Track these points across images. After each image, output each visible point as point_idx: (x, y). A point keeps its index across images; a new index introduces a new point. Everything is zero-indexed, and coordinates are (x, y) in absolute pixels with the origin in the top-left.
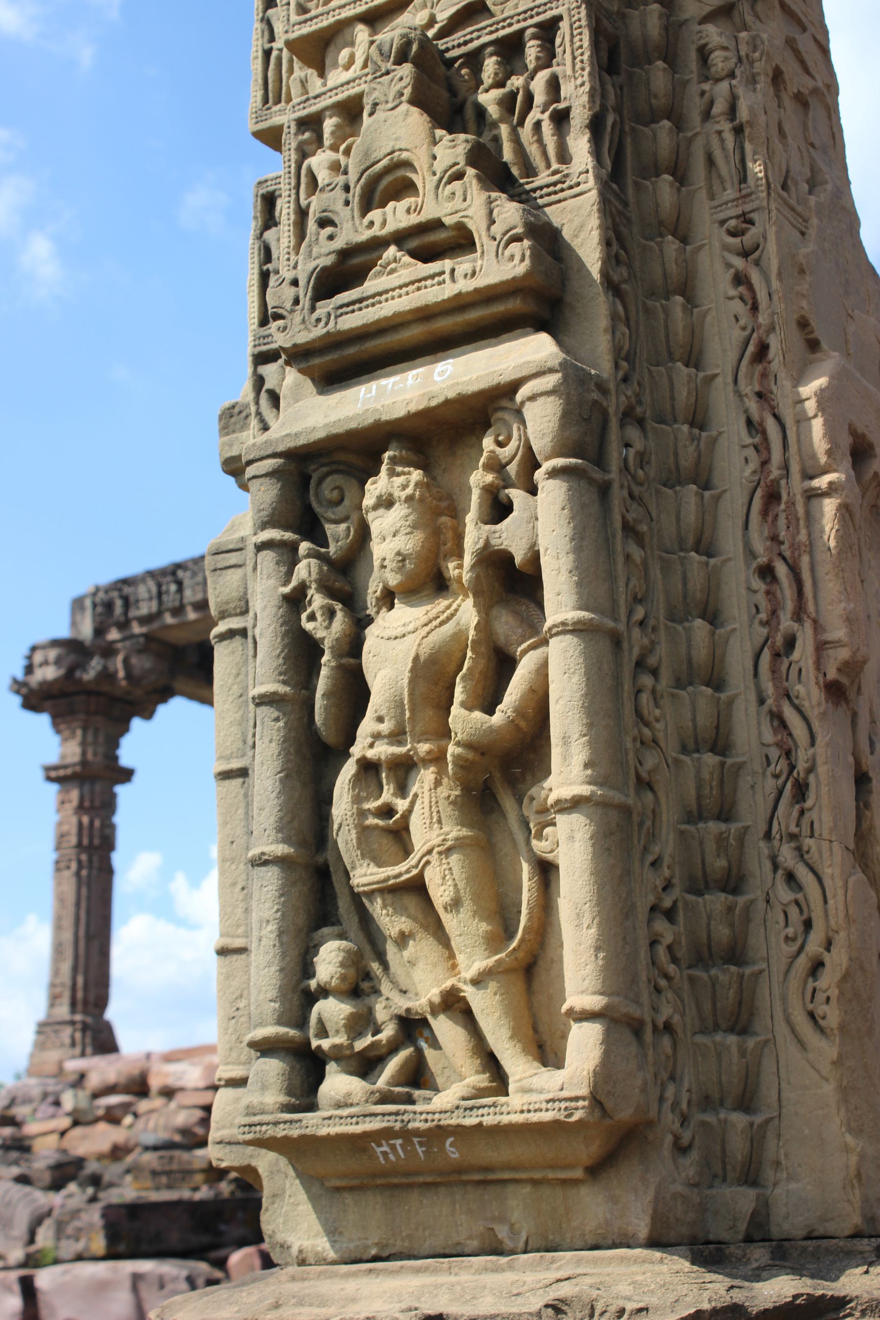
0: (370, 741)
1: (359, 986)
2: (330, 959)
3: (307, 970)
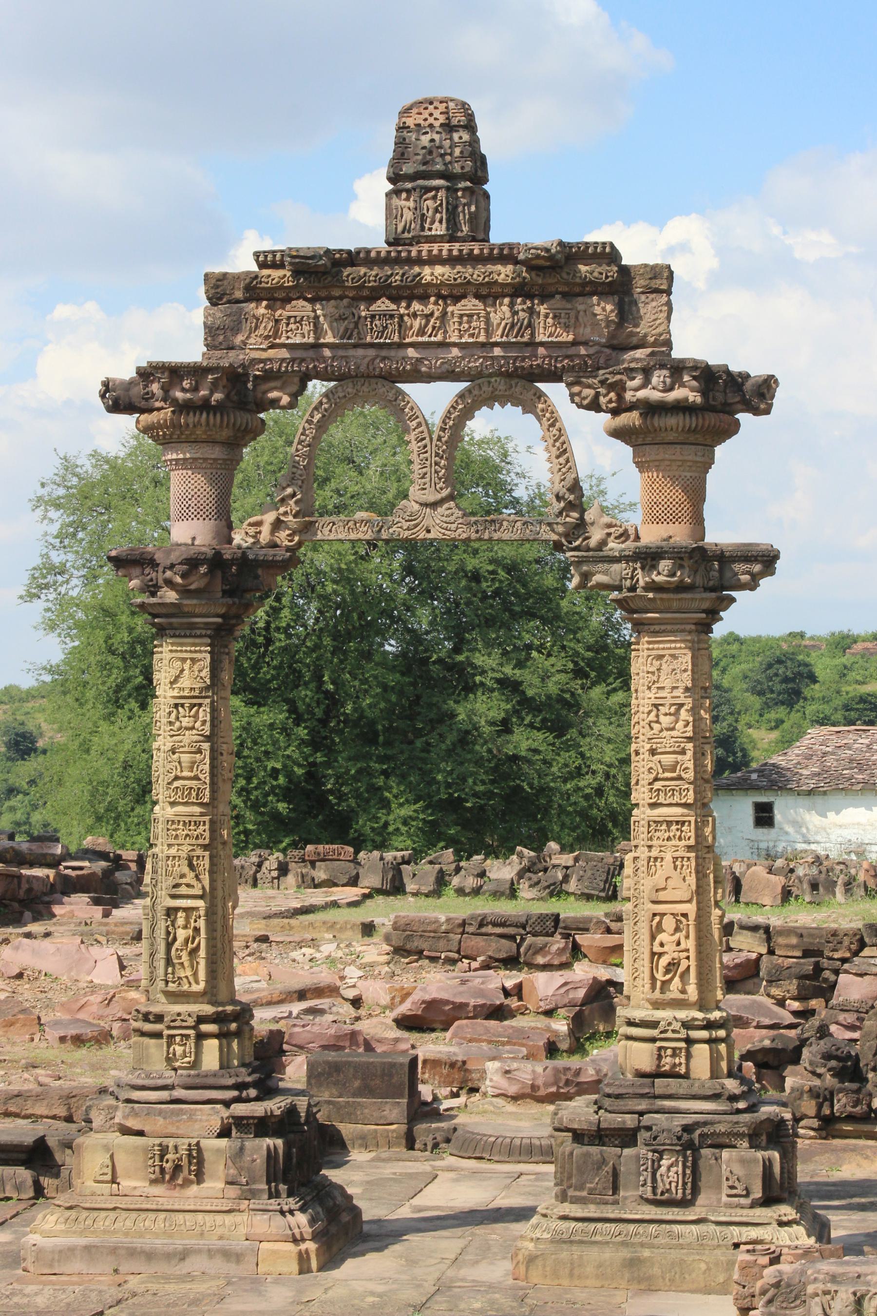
0: (177, 944)
1: (173, 973)
2: (170, 970)
3: (166, 970)
